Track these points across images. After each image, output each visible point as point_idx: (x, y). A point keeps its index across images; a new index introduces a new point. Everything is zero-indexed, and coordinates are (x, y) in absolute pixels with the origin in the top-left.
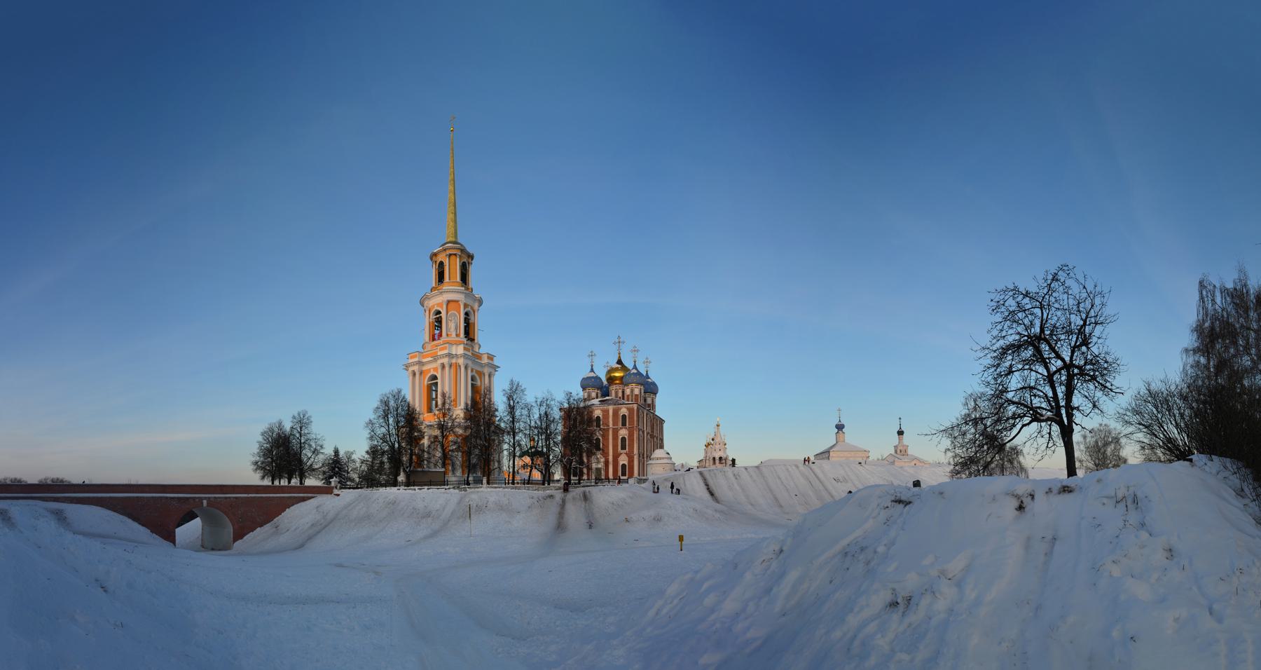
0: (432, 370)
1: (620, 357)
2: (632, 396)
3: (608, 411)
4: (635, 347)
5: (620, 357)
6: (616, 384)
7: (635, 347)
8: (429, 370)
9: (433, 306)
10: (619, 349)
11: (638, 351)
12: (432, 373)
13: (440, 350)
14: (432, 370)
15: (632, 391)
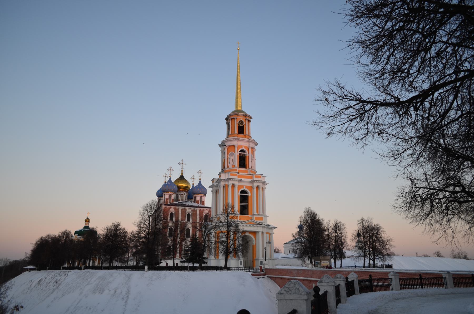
0: (244, 187)
1: (182, 173)
2: (201, 202)
3: (197, 211)
4: (200, 170)
5: (182, 173)
6: (182, 191)
7: (200, 170)
8: (243, 186)
9: (241, 147)
10: (182, 168)
11: (202, 173)
12: (244, 188)
13: (255, 177)
14: (244, 187)
15: (201, 198)
